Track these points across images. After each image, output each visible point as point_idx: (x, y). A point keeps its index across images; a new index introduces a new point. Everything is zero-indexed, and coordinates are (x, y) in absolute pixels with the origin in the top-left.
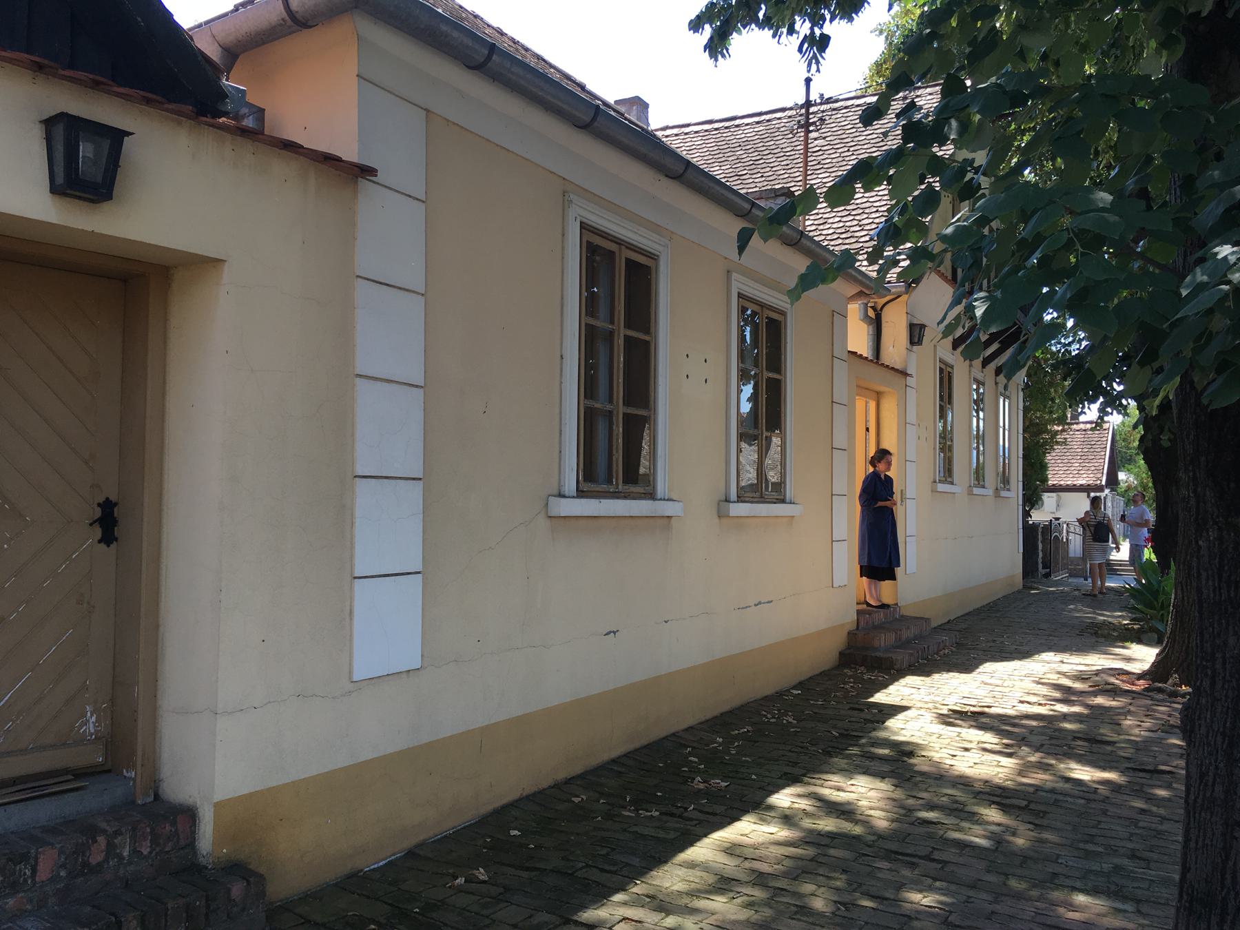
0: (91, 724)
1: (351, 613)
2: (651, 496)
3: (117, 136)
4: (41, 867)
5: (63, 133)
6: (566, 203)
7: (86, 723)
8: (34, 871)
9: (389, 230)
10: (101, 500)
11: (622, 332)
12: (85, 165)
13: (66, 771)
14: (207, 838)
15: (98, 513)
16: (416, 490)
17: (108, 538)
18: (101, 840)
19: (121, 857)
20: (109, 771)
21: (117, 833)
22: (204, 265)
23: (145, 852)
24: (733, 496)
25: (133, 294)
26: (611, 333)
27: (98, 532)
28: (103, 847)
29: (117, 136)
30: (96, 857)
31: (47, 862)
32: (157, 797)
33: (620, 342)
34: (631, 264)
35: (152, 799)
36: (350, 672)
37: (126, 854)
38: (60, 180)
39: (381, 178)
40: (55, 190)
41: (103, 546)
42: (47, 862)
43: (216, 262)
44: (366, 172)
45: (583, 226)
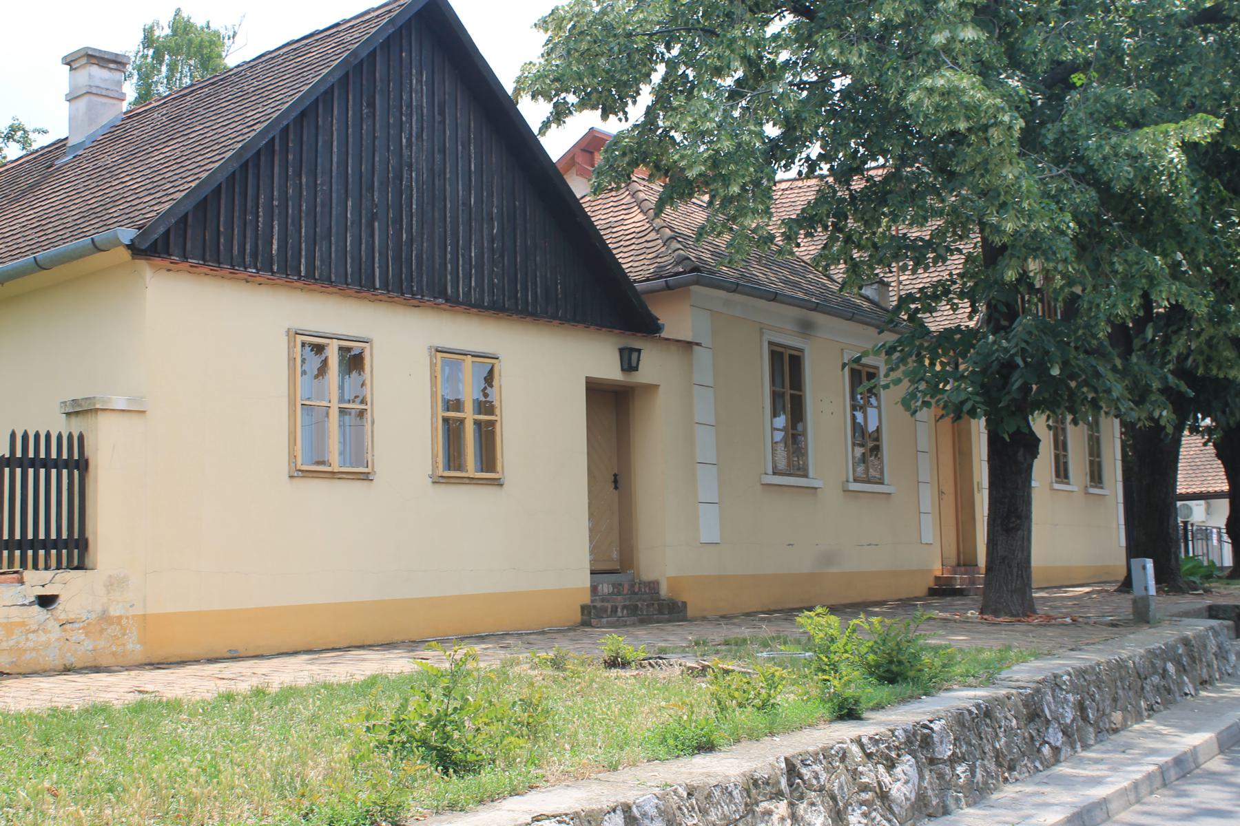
0: (615, 555)
2: (806, 476)
3: (639, 351)
6: (762, 334)
11: (789, 392)
12: (629, 361)
14: (664, 591)
16: (714, 468)
17: (616, 488)
22: (651, 388)
24: (851, 479)
26: (784, 393)
29: (639, 351)
33: (788, 398)
34: (791, 356)
38: (626, 366)
40: (623, 370)
43: (656, 387)
44: (698, 344)
45: (770, 343)
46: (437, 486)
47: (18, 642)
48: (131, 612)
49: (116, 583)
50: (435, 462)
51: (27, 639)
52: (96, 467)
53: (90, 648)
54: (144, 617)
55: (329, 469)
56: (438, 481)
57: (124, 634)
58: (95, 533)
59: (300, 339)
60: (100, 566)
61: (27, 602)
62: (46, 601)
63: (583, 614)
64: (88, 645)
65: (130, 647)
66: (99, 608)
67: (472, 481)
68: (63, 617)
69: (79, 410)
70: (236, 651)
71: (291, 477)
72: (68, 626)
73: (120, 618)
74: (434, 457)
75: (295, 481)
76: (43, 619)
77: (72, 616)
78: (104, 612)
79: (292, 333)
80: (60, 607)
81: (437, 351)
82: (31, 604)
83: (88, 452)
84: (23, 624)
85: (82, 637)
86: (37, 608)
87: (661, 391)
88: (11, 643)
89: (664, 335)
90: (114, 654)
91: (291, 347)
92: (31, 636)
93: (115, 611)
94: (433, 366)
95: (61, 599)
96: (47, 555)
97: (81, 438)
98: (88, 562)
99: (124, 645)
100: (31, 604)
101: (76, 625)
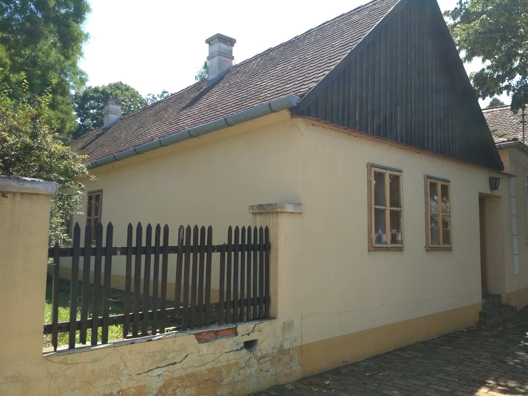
3: (499, 179)
5: (491, 179)
14: (504, 300)
29: (499, 179)
47: (234, 378)
49: (288, 326)
50: (427, 240)
51: (239, 374)
52: (277, 249)
53: (273, 373)
54: (301, 346)
56: (429, 249)
57: (291, 361)
58: (276, 293)
59: (373, 169)
60: (279, 316)
61: (238, 348)
62: (249, 345)
63: (480, 317)
64: (273, 371)
65: (294, 368)
66: (278, 345)
68: (259, 354)
69: (262, 210)
71: (369, 251)
72: (262, 360)
73: (289, 350)
76: (248, 359)
77: (264, 353)
78: (282, 346)
79: (369, 166)
80: (258, 348)
82: (242, 349)
83: (272, 239)
84: (237, 364)
85: (269, 366)
86: (244, 351)
88: (230, 378)
89: (505, 171)
90: (286, 375)
91: (369, 175)
92: (242, 372)
93: (286, 346)
95: (259, 342)
96: (249, 310)
97: (267, 229)
98: (272, 312)
99: (291, 368)
100: (242, 349)
101: (266, 359)
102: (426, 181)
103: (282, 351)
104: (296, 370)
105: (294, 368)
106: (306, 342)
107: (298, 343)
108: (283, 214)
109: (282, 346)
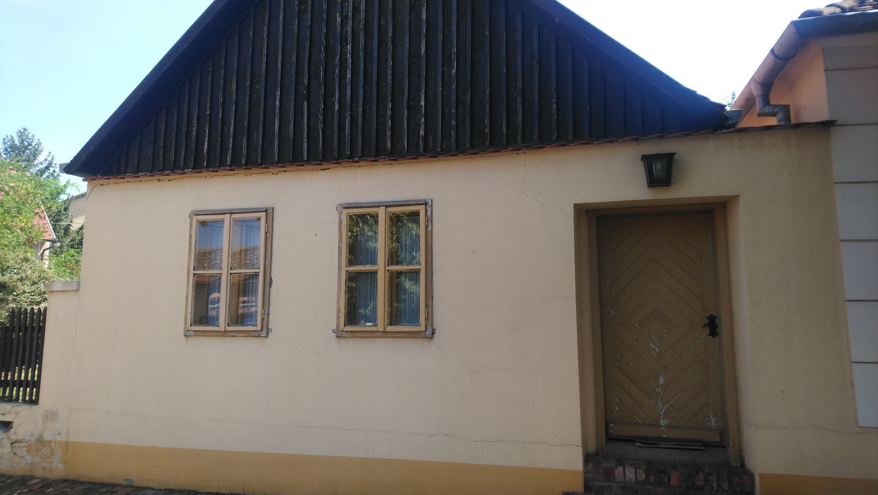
1: (852, 384)
3: (669, 158)
4: (672, 478)
7: (710, 421)
8: (669, 480)
9: (848, 155)
10: (708, 315)
12: (661, 171)
13: (700, 441)
15: (707, 321)
18: (701, 475)
19: (712, 487)
20: (724, 447)
21: (709, 474)
23: (726, 488)
25: (709, 218)
27: (708, 331)
28: (702, 478)
29: (669, 158)
30: (700, 482)
31: (675, 478)
32: (743, 465)
35: (739, 465)
36: (857, 423)
37: (715, 485)
39: (838, 123)
41: (711, 337)
42: (675, 478)
46: (341, 340)
48: (58, 438)
49: (50, 416)
53: (29, 462)
54: (67, 444)
55: (216, 329)
56: (340, 335)
57: (52, 455)
64: (29, 459)
65: (55, 465)
66: (37, 434)
67: (385, 334)
68: (14, 437)
70: (131, 480)
72: (17, 444)
73: (50, 442)
74: (339, 311)
75: (190, 339)
77: (20, 437)
78: (41, 436)
81: (345, 208)
85: (25, 453)
87: (742, 202)
90: (44, 468)
93: (48, 437)
94: (340, 221)
95: (15, 424)
99: (51, 463)
101: (22, 444)
102: (340, 213)
103: (40, 441)
104: (57, 468)
105: (55, 465)
106: (73, 438)
107: (63, 438)
108: (55, 294)
109: (41, 436)
